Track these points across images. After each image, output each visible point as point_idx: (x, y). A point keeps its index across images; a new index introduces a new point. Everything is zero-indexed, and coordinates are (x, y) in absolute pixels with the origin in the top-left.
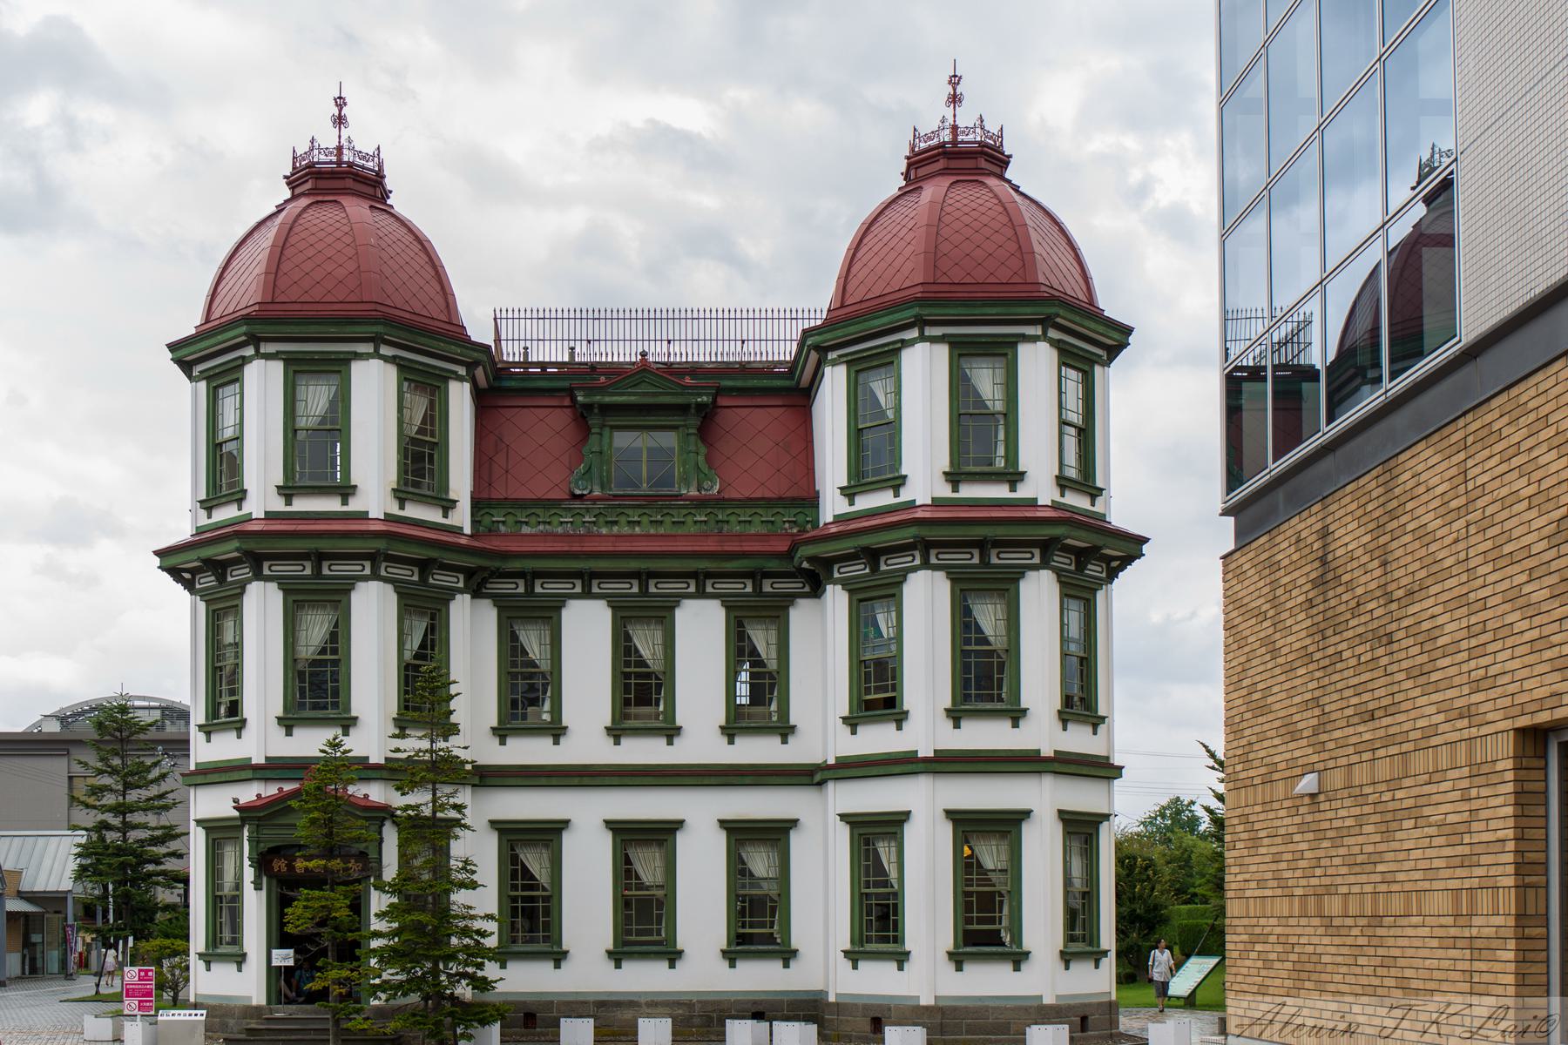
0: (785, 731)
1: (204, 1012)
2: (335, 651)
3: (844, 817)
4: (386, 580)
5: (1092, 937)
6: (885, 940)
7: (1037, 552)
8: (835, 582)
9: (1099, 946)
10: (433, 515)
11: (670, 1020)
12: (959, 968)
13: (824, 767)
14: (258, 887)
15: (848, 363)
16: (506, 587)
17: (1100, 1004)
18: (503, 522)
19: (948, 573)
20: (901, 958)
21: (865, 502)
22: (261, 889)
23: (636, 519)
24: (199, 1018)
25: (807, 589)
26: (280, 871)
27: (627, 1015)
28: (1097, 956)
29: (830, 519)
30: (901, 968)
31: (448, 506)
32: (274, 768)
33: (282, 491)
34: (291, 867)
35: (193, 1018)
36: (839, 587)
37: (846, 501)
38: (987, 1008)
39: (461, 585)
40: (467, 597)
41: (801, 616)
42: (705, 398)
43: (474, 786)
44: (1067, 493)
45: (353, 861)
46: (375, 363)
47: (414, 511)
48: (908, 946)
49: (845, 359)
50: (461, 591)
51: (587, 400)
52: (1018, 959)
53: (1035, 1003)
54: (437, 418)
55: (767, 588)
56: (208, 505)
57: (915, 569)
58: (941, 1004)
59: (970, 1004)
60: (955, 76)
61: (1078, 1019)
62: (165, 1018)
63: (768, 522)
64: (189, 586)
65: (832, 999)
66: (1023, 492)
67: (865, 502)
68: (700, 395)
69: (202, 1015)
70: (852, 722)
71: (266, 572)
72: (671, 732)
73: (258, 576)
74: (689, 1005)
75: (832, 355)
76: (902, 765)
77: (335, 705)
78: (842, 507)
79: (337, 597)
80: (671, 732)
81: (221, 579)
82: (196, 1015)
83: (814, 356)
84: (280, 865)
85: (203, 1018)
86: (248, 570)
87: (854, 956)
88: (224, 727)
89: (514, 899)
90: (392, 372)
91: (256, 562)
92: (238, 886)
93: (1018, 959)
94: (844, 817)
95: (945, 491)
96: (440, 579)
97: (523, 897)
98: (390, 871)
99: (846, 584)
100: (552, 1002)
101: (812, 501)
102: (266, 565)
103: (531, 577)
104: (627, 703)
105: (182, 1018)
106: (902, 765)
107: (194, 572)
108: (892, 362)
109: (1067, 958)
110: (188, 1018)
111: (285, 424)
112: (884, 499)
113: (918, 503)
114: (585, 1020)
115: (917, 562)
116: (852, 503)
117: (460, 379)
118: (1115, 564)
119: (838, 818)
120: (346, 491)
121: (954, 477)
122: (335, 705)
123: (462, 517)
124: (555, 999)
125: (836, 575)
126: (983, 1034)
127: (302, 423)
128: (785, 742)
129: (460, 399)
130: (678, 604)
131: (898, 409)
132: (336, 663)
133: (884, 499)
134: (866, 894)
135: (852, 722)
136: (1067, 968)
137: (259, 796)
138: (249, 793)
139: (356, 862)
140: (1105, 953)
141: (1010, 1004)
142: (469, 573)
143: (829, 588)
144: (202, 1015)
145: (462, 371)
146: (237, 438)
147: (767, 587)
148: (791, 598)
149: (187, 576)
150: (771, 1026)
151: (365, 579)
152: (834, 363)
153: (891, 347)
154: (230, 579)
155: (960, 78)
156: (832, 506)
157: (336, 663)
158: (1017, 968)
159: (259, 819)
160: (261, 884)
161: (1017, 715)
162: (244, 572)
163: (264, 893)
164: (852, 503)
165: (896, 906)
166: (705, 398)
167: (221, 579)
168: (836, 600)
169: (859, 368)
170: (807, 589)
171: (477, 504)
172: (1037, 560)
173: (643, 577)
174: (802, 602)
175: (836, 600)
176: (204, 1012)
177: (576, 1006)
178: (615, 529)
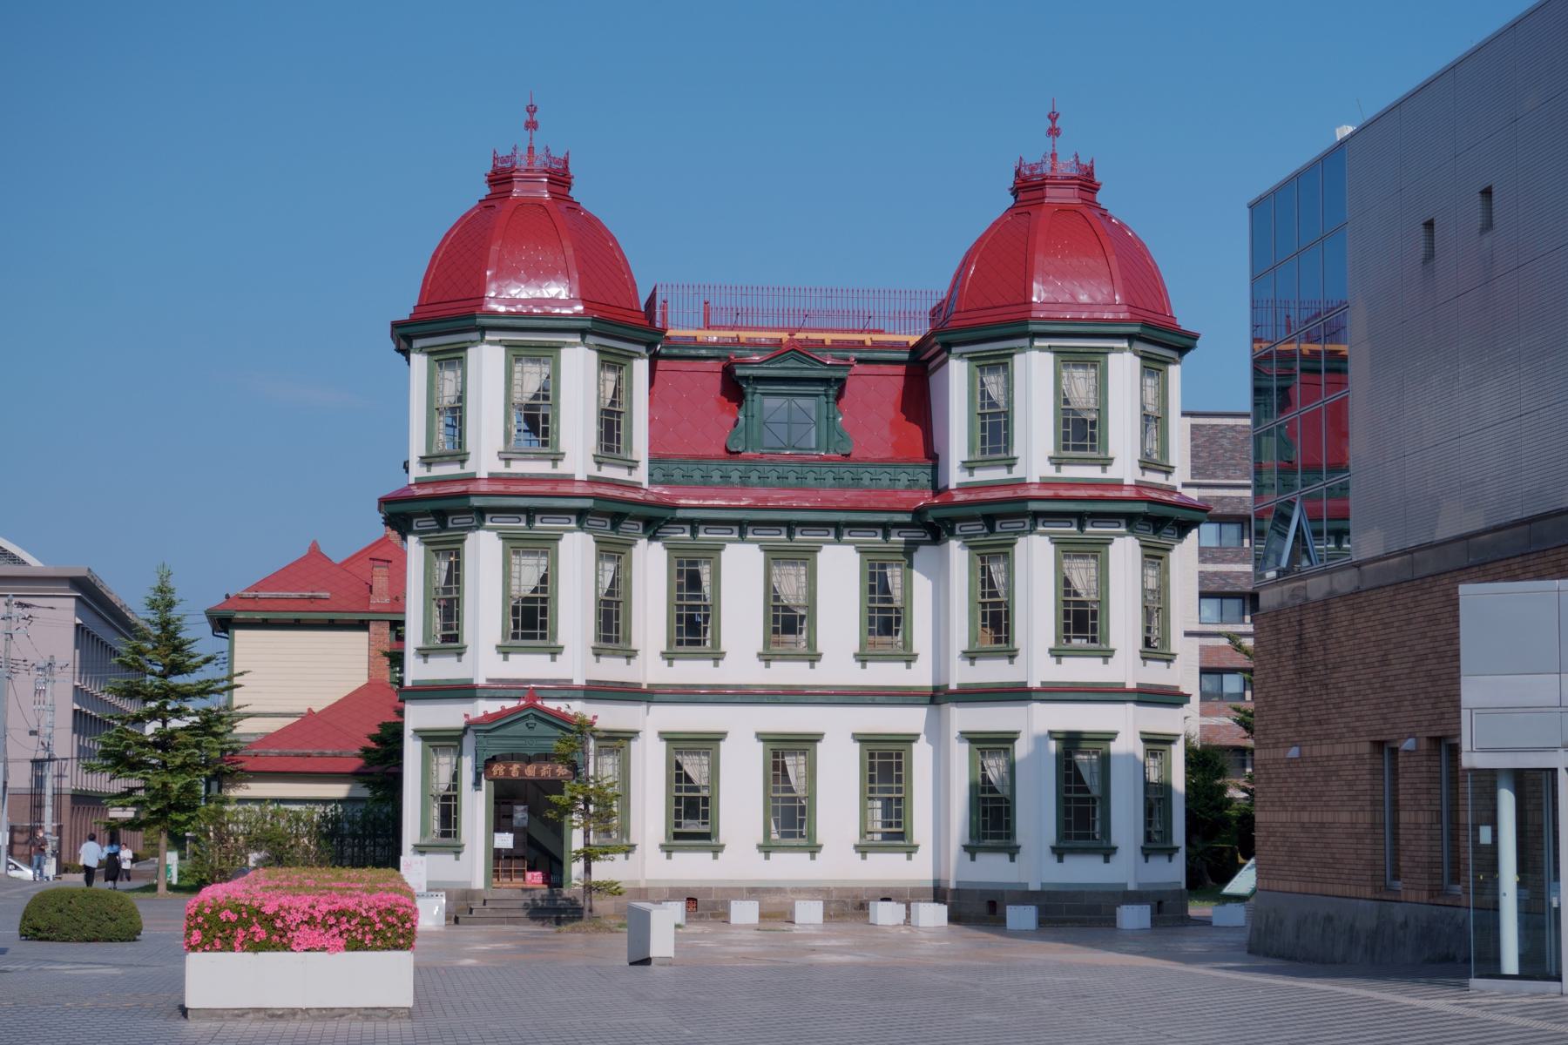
2: (544, 590)
6: (999, 836)
10: (620, 474)
12: (1060, 860)
17: (1173, 892)
19: (1051, 539)
20: (1013, 851)
22: (481, 790)
28: (1170, 852)
30: (1012, 860)
31: (632, 466)
32: (497, 689)
34: (507, 772)
44: (1147, 473)
46: (582, 350)
47: (609, 472)
52: (1108, 852)
54: (621, 392)
58: (1046, 889)
61: (1156, 903)
67: (982, 476)
70: (971, 656)
72: (813, 657)
76: (1017, 694)
77: (543, 637)
79: (546, 545)
80: (813, 657)
89: (775, 800)
90: (594, 355)
93: (1108, 852)
97: (783, 798)
104: (775, 631)
106: (1017, 694)
109: (1147, 852)
112: (999, 474)
115: (1027, 527)
123: (641, 475)
131: (1010, 401)
132: (544, 600)
133: (999, 474)
134: (983, 798)
136: (1147, 861)
140: (1176, 849)
150: (908, 908)
153: (1006, 352)
155: (1058, 115)
156: (956, 476)
157: (544, 600)
158: (1107, 861)
159: (488, 731)
165: (1008, 809)
173: (790, 527)
175: (957, 554)
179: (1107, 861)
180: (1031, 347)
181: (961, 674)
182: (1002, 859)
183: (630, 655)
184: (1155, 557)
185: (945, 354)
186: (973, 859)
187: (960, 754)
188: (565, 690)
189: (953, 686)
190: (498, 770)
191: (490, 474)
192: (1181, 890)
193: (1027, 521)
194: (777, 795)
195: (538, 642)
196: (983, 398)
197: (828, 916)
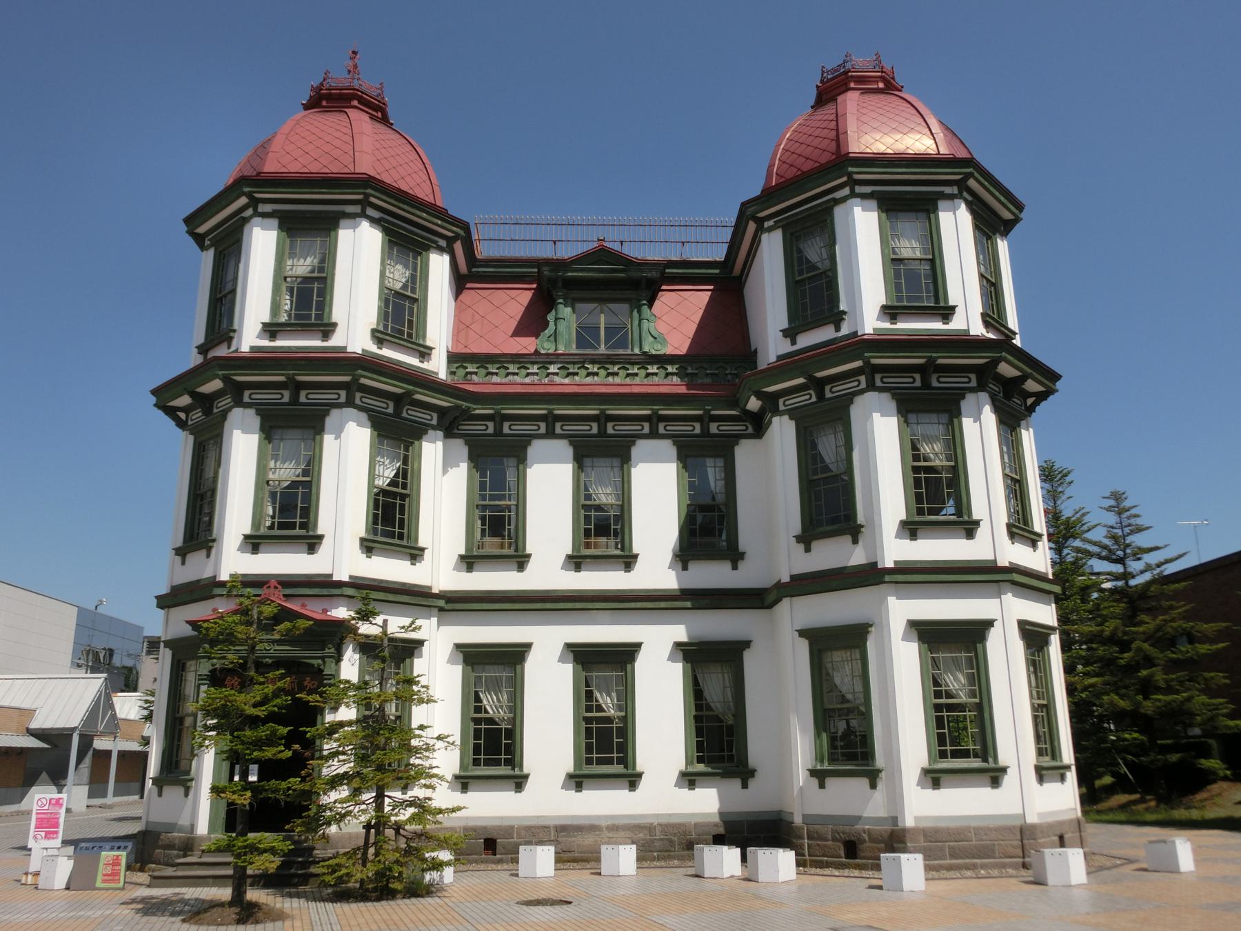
0: (734, 556)
3: (803, 633)
4: (360, 409)
5: (1055, 753)
7: (973, 377)
8: (781, 413)
9: (1061, 761)
11: (634, 847)
13: (779, 585)
16: (476, 428)
18: (476, 373)
20: (873, 777)
21: (807, 340)
27: (588, 840)
29: (773, 359)
36: (786, 417)
37: (788, 340)
38: (968, 829)
39: (434, 422)
40: (440, 434)
41: (745, 453)
43: (441, 609)
45: (308, 679)
49: (781, 224)
50: (434, 428)
52: (995, 776)
53: (1018, 823)
57: (861, 392)
59: (953, 825)
61: (1056, 838)
64: (182, 424)
66: (957, 323)
67: (807, 340)
70: (806, 539)
71: (246, 399)
73: (239, 403)
74: (650, 828)
75: (766, 224)
78: (785, 347)
81: (208, 412)
83: (752, 226)
86: (229, 400)
87: (819, 776)
88: (197, 548)
91: (236, 392)
94: (803, 633)
96: (410, 413)
99: (792, 413)
100: (512, 827)
101: (750, 356)
102: (247, 393)
104: (587, 533)
107: (186, 410)
108: (826, 220)
111: (275, 271)
112: (824, 334)
114: (546, 848)
115: (863, 385)
116: (794, 343)
117: (441, 250)
118: (1030, 401)
119: (797, 634)
122: (304, 526)
124: (516, 823)
125: (782, 408)
126: (968, 858)
128: (735, 568)
129: (439, 266)
133: (824, 334)
135: (806, 539)
139: (312, 680)
141: (992, 824)
143: (776, 420)
145: (443, 243)
147: (713, 428)
149: (182, 415)
151: (340, 406)
152: (770, 229)
154: (215, 411)
161: (969, 528)
162: (226, 401)
164: (794, 343)
168: (783, 431)
170: (750, 430)
171: (455, 359)
172: (974, 384)
175: (783, 431)
177: (537, 833)
178: (577, 378)
183: (415, 555)
184: (1010, 422)
188: (324, 586)
191: (252, 348)
192: (1079, 821)
193: (863, 378)
195: (297, 532)
196: (800, 264)
197: (643, 858)
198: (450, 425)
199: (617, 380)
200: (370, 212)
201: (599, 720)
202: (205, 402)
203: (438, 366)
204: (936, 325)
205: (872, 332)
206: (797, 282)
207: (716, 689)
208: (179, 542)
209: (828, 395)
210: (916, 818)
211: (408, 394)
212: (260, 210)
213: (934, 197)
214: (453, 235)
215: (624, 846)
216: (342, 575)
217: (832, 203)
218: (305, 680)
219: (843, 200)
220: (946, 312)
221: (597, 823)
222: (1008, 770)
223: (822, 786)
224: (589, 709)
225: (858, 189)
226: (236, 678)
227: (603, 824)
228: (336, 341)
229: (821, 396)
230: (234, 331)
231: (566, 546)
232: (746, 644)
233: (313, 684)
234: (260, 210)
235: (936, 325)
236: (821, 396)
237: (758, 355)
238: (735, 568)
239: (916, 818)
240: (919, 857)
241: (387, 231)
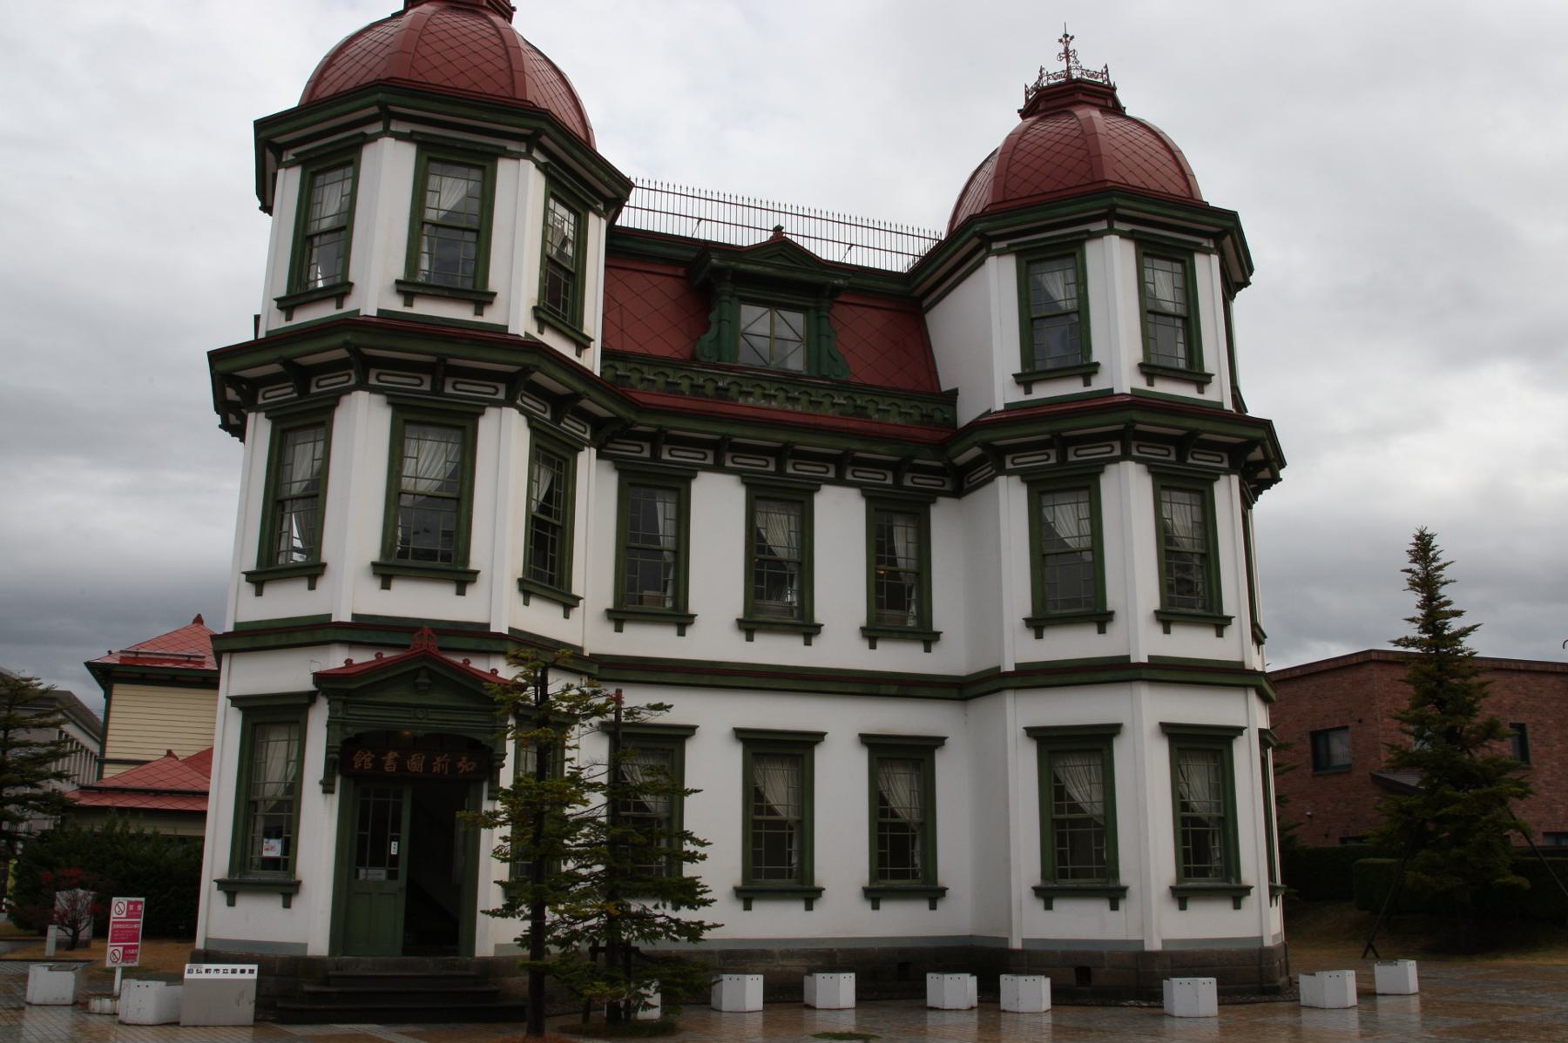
0: (928, 637)
1: (255, 967)
3: (1032, 732)
10: (566, 349)
14: (327, 787)
15: (1020, 255)
16: (629, 450)
22: (332, 792)
23: (773, 392)
24: (247, 976)
25: (947, 487)
26: (362, 767)
31: (582, 343)
32: (364, 629)
33: (402, 288)
34: (378, 763)
35: (238, 976)
42: (841, 282)
45: (464, 759)
48: (1124, 879)
49: (1016, 249)
51: (722, 264)
55: (907, 482)
56: (287, 305)
57: (1116, 460)
60: (1066, 36)
62: (194, 976)
63: (905, 413)
65: (1016, 944)
67: (1042, 392)
68: (838, 277)
69: (251, 971)
70: (1038, 624)
73: (362, 385)
78: (1017, 395)
80: (809, 630)
81: (303, 390)
82: (243, 971)
84: (363, 760)
85: (254, 976)
87: (1047, 894)
92: (294, 789)
94: (1032, 732)
95: (1141, 384)
98: (506, 779)
102: (373, 373)
103: (657, 439)
105: (221, 976)
110: (230, 976)
113: (1116, 392)
115: (1117, 452)
120: (482, 298)
121: (1149, 370)
123: (592, 360)
125: (1009, 466)
127: (431, 215)
128: (928, 650)
130: (818, 489)
137: (348, 662)
138: (335, 659)
139: (469, 761)
142: (597, 424)
144: (251, 971)
146: (343, 228)
148: (930, 497)
159: (349, 692)
160: (333, 785)
163: (335, 799)
164: (1028, 392)
166: (841, 282)
167: (303, 390)
169: (1030, 260)
171: (607, 355)
174: (942, 501)
176: (255, 967)
178: (751, 400)
179: (1237, 906)
180: (1111, 231)
181: (1021, 649)
182: (1100, 907)
185: (983, 252)
186: (1048, 907)
187: (1024, 765)
188: (479, 637)
189: (1009, 667)
190: (363, 760)
194: (760, 817)
195: (438, 564)
198: (607, 439)
199: (799, 408)
200: (536, 154)
201: (770, 824)
202: (300, 375)
203: (592, 360)
204: (1187, 391)
205: (1129, 392)
206: (1033, 320)
207: (902, 794)
208: (251, 564)
209: (1072, 458)
210: (1164, 942)
211: (577, 396)
212: (393, 128)
213: (1193, 248)
214: (614, 196)
215: (730, 976)
216: (500, 626)
217: (1085, 236)
218: (460, 760)
219: (1099, 235)
220: (1202, 380)
221: (769, 948)
222: (1252, 890)
223: (1048, 907)
224: (759, 810)
225: (1118, 226)
226: (369, 754)
227: (776, 948)
228: (491, 316)
229: (1062, 458)
230: (351, 285)
231: (735, 605)
232: (939, 741)
233: (470, 767)
234: (393, 128)
235: (1187, 391)
236: (1062, 458)
237: (959, 397)
238: (928, 650)
239: (1164, 942)
240: (1213, 980)
241: (551, 180)
